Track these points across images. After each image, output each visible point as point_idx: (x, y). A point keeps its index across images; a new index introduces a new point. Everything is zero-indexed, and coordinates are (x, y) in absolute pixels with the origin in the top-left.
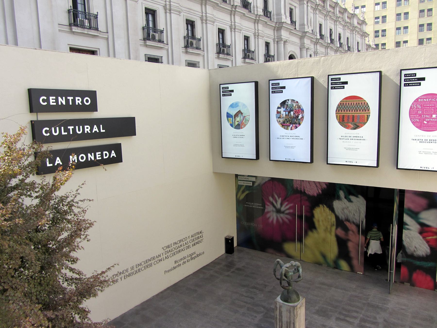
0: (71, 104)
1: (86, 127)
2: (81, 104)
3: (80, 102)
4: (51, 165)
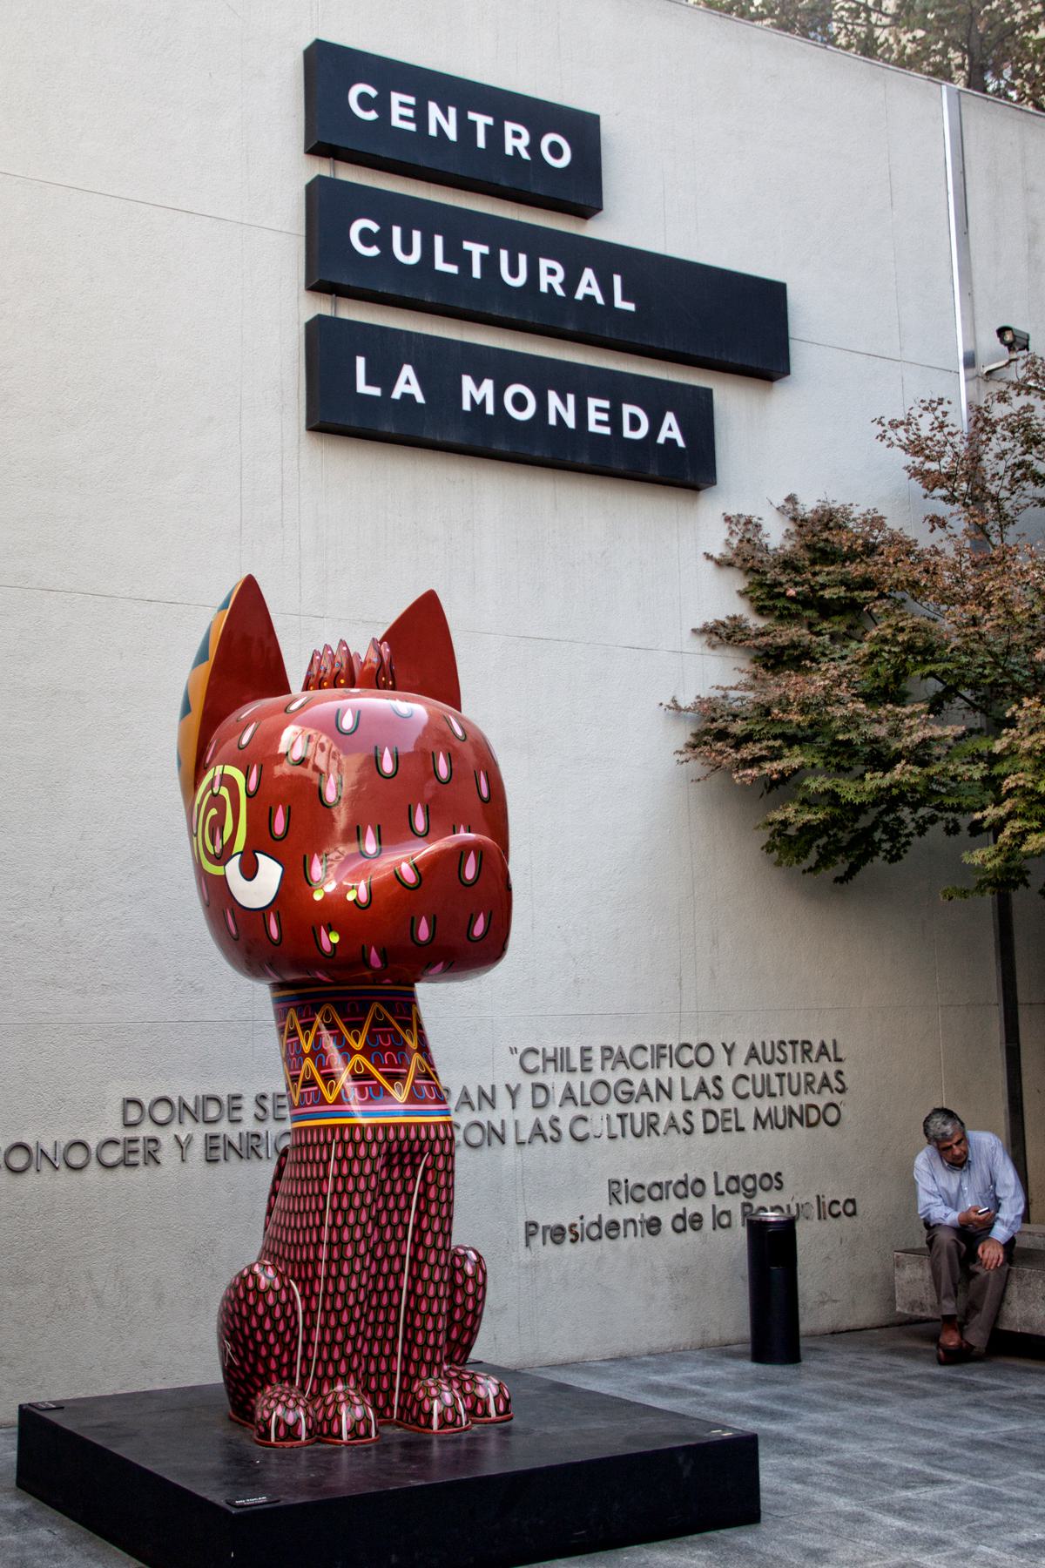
2: (525, 155)
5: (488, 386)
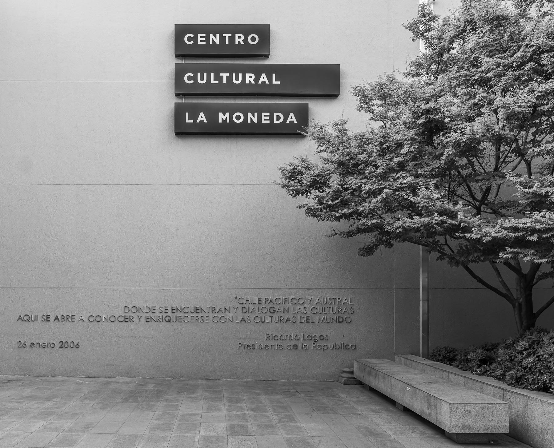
0: (227, 43)
2: (242, 43)
3: (241, 40)
4: (192, 121)
5: (228, 115)
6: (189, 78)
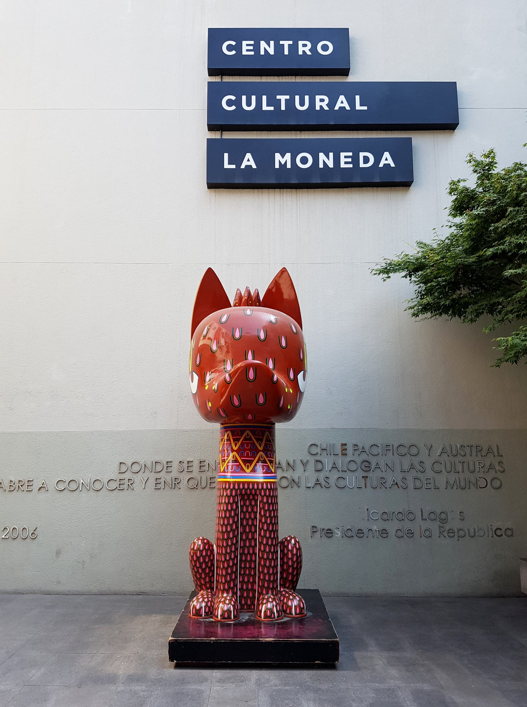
0: (286, 52)
1: (318, 98)
3: (307, 50)
4: (234, 167)
5: (288, 156)
6: (230, 103)
